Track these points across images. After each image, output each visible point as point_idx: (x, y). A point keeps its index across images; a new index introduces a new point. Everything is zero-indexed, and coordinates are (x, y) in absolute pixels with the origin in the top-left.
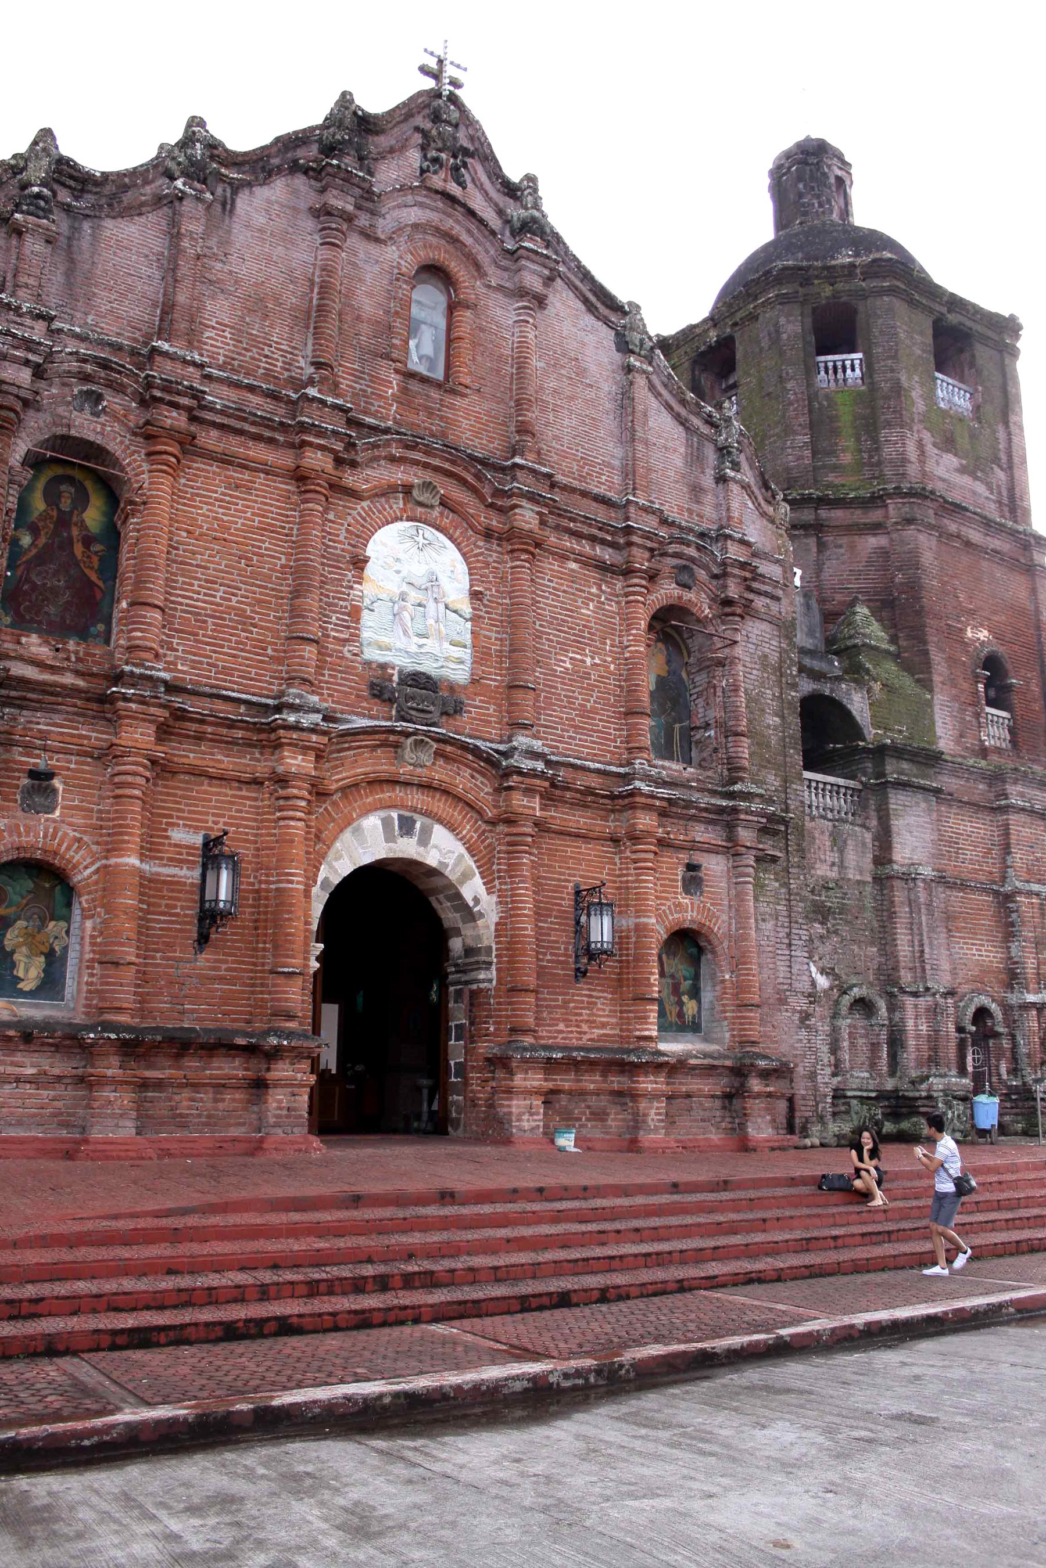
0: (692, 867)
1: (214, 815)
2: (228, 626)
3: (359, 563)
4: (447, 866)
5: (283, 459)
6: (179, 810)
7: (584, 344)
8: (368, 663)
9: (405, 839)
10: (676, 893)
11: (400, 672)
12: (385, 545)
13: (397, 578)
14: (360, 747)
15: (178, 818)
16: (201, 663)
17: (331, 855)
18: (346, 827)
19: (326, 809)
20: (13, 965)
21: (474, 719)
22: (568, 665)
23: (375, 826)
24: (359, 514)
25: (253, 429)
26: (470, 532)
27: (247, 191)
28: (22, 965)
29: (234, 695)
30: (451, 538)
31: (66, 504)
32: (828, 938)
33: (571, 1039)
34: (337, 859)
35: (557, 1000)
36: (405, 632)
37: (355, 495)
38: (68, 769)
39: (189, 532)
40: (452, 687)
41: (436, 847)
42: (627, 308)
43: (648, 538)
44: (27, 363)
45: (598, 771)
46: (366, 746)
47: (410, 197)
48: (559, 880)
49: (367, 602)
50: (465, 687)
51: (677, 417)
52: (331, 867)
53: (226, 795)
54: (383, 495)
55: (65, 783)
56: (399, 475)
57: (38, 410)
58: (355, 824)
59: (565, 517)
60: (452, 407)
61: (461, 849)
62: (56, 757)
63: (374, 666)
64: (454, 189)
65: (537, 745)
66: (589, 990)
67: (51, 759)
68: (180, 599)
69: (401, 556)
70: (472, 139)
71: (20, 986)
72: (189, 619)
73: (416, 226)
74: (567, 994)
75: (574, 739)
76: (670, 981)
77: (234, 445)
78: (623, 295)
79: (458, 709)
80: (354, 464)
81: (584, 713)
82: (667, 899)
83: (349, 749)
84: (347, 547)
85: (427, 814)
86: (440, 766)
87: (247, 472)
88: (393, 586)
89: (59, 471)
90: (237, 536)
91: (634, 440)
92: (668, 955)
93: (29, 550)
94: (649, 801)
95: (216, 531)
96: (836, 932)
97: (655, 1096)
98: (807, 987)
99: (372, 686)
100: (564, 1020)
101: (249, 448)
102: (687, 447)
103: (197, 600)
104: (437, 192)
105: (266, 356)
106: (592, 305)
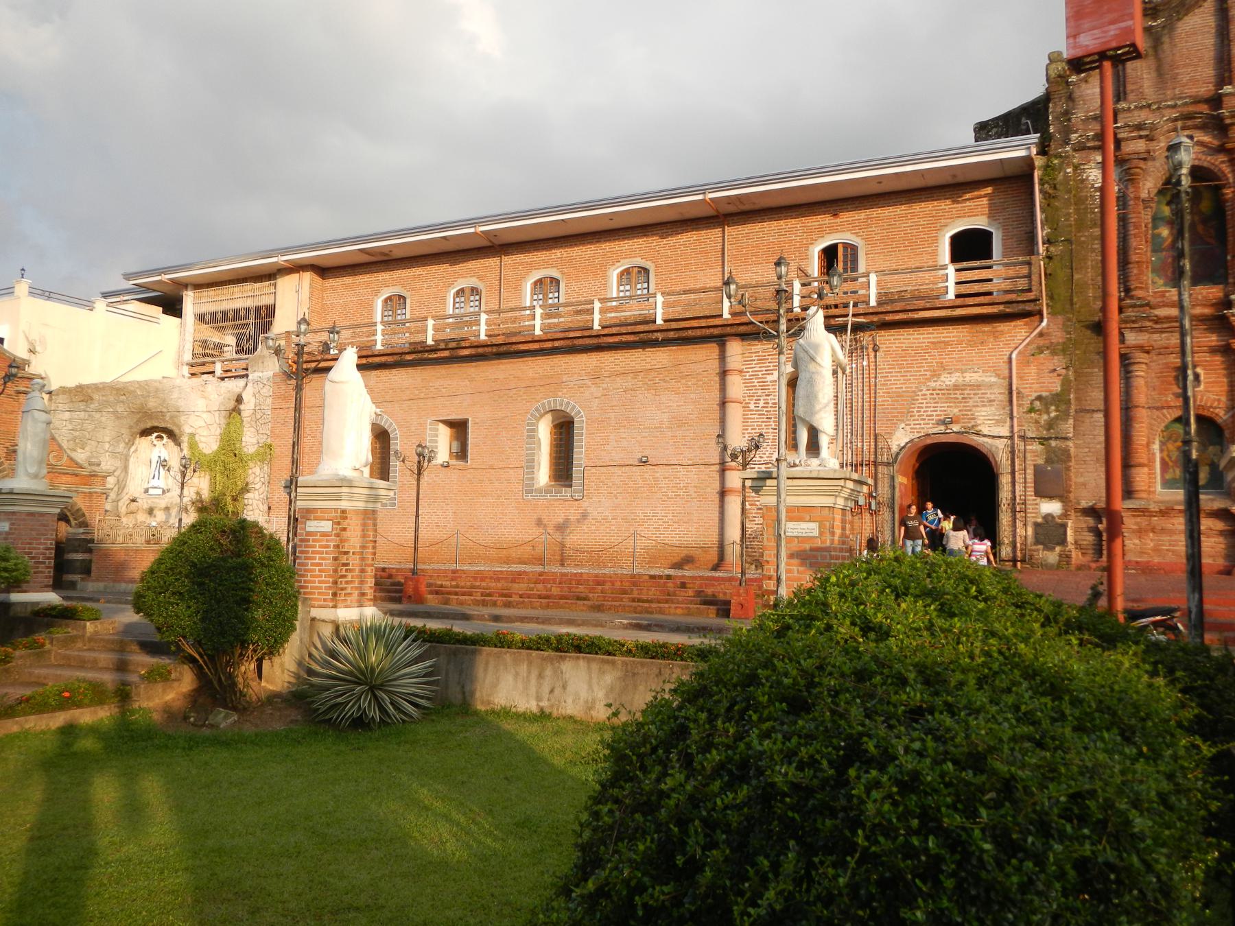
44: (1141, 137)
55: (1205, 369)
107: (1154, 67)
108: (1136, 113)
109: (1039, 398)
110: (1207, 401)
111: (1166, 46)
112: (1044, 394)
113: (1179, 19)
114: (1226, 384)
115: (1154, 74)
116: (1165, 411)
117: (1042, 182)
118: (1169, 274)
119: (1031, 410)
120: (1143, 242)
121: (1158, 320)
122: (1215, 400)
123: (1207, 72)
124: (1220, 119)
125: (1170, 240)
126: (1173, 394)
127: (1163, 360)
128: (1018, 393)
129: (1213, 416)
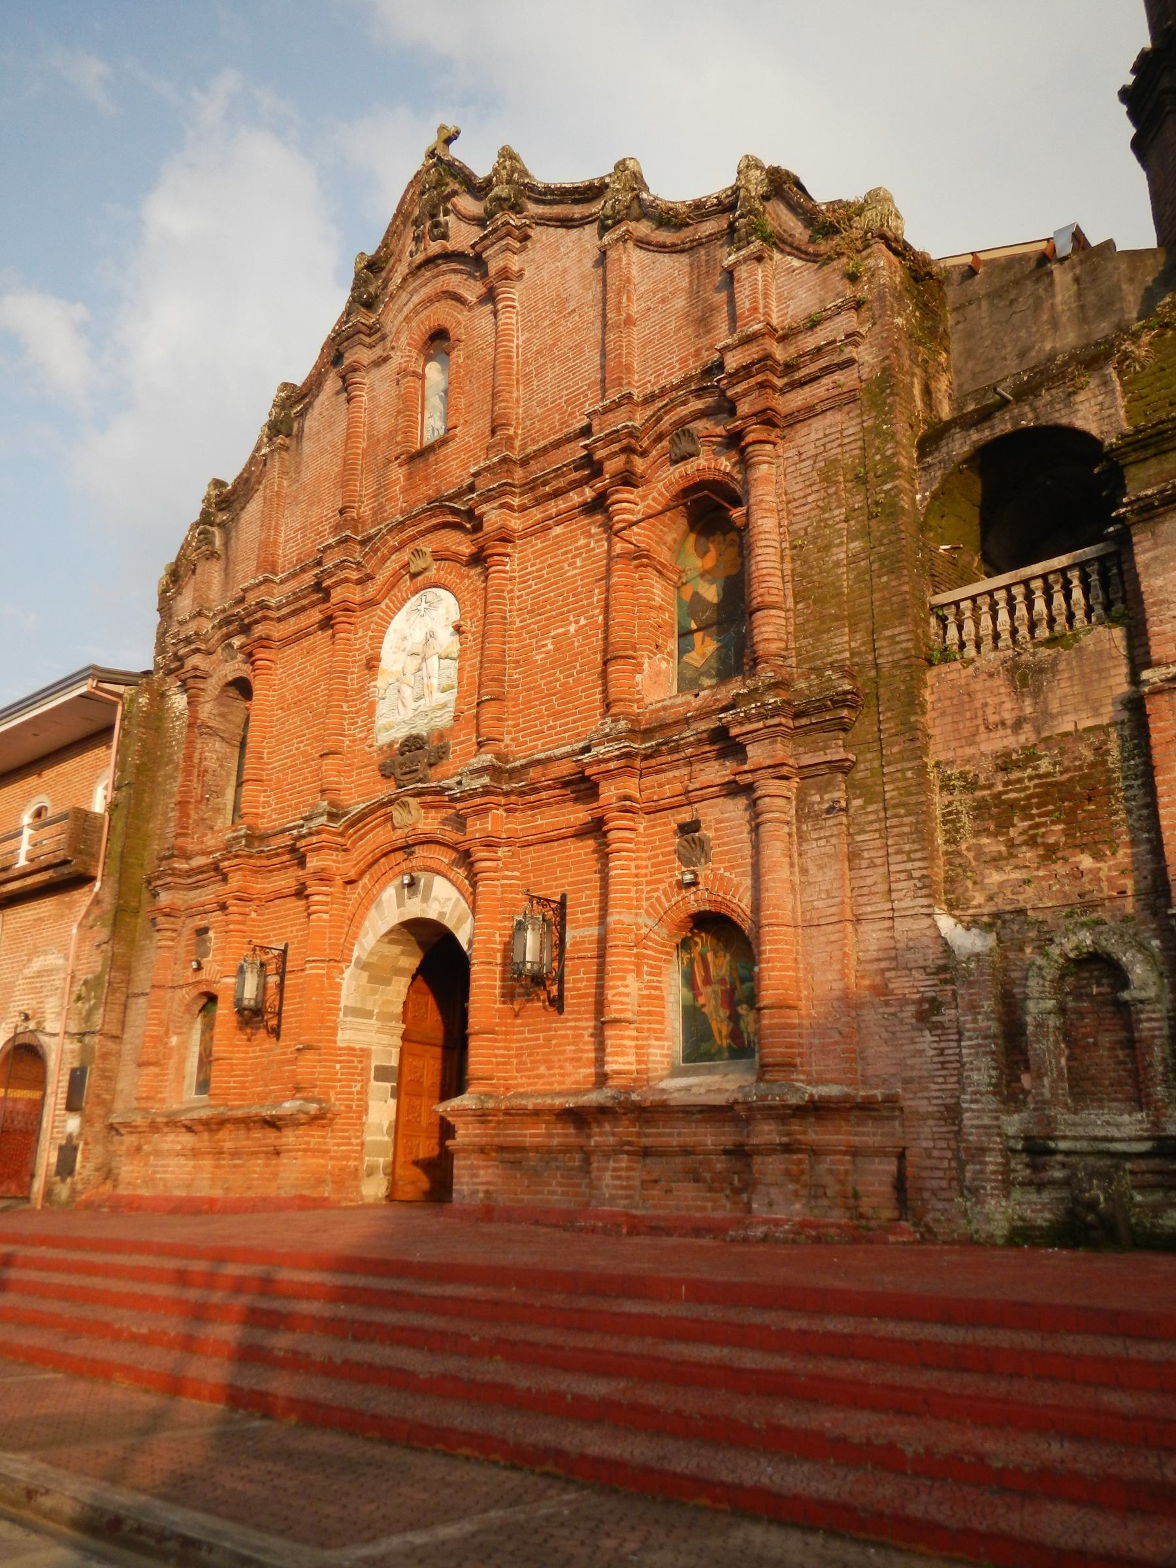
0: (688, 829)
3: (372, 664)
8: (381, 748)
17: (362, 933)
18: (370, 904)
22: (550, 647)
23: (391, 896)
32: (1012, 856)
33: (551, 1084)
35: (537, 1039)
37: (371, 603)
39: (282, 708)
40: (441, 736)
41: (436, 899)
43: (612, 442)
49: (382, 691)
50: (451, 729)
52: (361, 944)
54: (393, 586)
66: (575, 1020)
73: (407, 319)
74: (550, 1029)
76: (718, 988)
79: (442, 753)
80: (370, 577)
82: (661, 881)
85: (427, 869)
86: (433, 818)
92: (716, 956)
94: (603, 767)
96: (1032, 842)
98: (933, 957)
100: (546, 1061)
101: (310, 617)
109: (86, 983)
111: (233, 541)
112: (90, 976)
113: (243, 508)
116: (184, 990)
117: (123, 720)
119: (79, 998)
121: (190, 873)
128: (73, 977)
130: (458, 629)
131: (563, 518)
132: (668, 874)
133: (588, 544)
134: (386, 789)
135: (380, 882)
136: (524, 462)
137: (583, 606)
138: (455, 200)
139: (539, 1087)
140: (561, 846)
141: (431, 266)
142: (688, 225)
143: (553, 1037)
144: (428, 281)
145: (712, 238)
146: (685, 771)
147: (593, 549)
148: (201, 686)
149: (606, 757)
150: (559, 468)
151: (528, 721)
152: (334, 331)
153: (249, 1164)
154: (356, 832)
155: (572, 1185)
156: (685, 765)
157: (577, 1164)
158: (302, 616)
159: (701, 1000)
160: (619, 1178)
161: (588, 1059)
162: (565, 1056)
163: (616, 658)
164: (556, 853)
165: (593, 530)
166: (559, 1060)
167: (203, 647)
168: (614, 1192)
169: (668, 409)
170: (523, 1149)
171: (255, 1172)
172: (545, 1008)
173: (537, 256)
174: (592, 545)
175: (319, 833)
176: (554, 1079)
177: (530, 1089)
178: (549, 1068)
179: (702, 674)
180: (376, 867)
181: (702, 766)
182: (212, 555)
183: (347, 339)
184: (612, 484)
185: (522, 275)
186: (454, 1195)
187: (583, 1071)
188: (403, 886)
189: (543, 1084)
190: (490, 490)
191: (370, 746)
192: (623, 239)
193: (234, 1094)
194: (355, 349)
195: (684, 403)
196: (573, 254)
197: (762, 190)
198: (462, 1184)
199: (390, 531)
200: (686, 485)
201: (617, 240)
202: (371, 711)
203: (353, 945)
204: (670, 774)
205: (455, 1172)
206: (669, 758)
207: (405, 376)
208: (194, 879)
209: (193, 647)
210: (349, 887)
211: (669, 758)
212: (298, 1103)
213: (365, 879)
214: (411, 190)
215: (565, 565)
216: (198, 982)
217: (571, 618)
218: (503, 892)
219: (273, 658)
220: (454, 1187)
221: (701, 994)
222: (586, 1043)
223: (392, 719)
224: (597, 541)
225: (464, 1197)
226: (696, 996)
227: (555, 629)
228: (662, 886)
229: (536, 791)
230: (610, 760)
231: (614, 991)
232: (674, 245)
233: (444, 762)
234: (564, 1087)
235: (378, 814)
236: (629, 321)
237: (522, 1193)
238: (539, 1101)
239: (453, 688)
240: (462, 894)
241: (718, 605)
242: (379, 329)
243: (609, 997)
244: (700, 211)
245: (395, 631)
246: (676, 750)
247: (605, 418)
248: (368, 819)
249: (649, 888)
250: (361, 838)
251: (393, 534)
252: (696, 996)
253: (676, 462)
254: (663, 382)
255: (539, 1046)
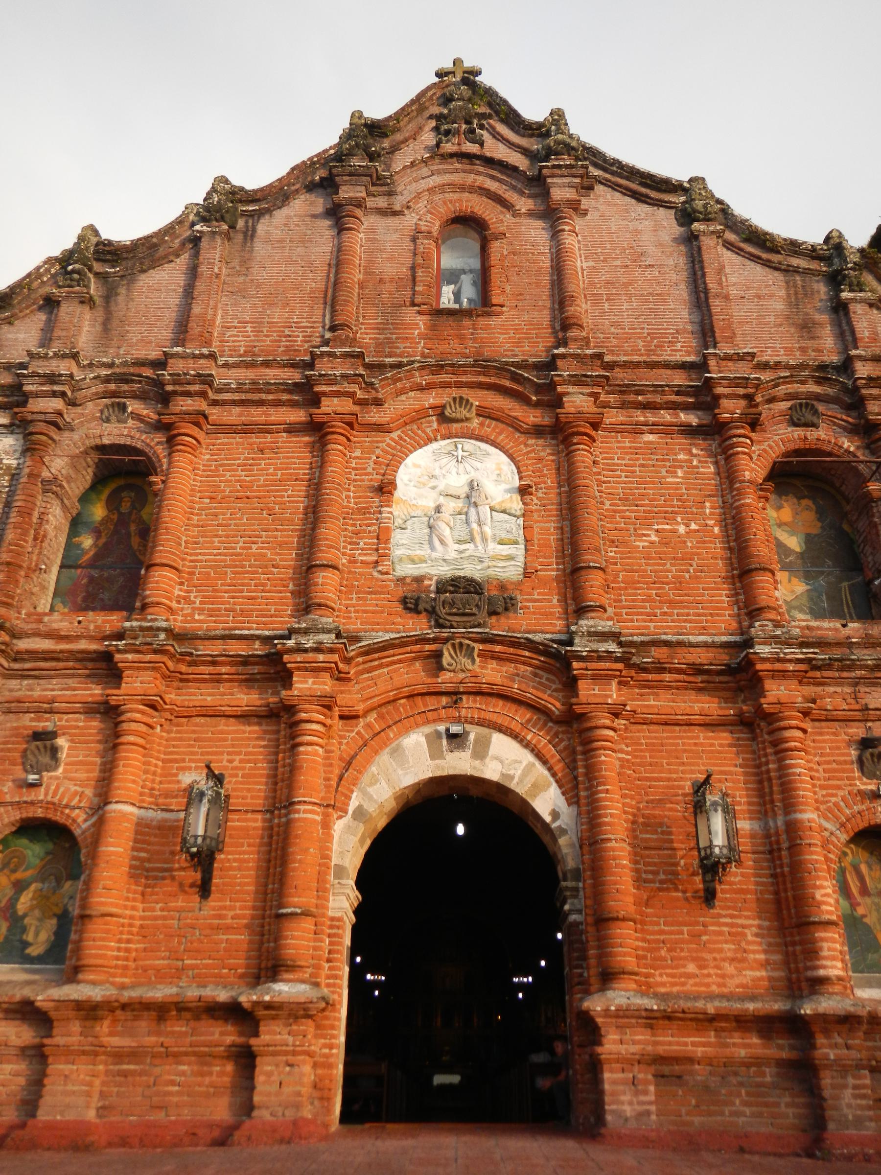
1: (229, 753)
2: (248, 572)
4: (512, 778)
5: (299, 416)
6: (193, 753)
7: (637, 232)
8: (401, 580)
9: (457, 754)
10: (854, 779)
11: (438, 583)
12: (418, 466)
13: (434, 494)
14: (394, 663)
15: (191, 761)
16: (219, 610)
17: (365, 779)
18: (381, 748)
19: (358, 733)
20: (24, 930)
21: (534, 613)
22: (654, 538)
23: (418, 743)
24: (388, 445)
25: (271, 397)
26: (517, 435)
27: (267, 217)
28: (33, 929)
29: (246, 632)
30: (494, 444)
31: (125, 507)
33: (708, 985)
34: (371, 784)
35: (682, 933)
36: (442, 542)
37: (381, 428)
38: (78, 727)
39: (211, 498)
40: (502, 586)
41: (497, 758)
42: (686, 185)
44: (54, 394)
45: (706, 645)
46: (400, 661)
47: (425, 169)
48: (669, 779)
49: (398, 522)
50: (520, 583)
51: (767, 264)
52: (365, 793)
53: (244, 732)
54: (413, 421)
55: (72, 741)
56: (431, 399)
57: (73, 430)
58: (394, 745)
59: (630, 392)
60: (487, 328)
61: (527, 757)
62: (65, 717)
63: (408, 581)
64: (471, 148)
65: (604, 625)
66: (732, 916)
67: (60, 720)
68: (200, 557)
69: (437, 472)
70: (490, 105)
71: (28, 951)
72: (208, 574)
74: (697, 923)
75: (671, 615)
77: (256, 415)
78: (680, 174)
80: (378, 402)
81: (679, 584)
82: (839, 787)
83: (381, 666)
84: (375, 476)
85: (481, 723)
86: (492, 669)
87: (269, 436)
88: (429, 502)
89: (121, 482)
90: (259, 491)
91: (707, 298)
92: (870, 867)
93: (90, 550)
94: (778, 666)
95: (238, 491)
97: (844, 1069)
99: (404, 601)
100: (694, 959)
101: (270, 415)
102: (788, 287)
103: (220, 554)
104: (452, 155)
105: (286, 336)
106: (642, 195)
107: (100, 320)
108: (54, 363)
110: (63, 795)
111: (121, 299)
113: (143, 271)
114: (98, 768)
115: (99, 328)
118: (79, 599)
120: (30, 539)
122: (76, 793)
123: (164, 333)
124: (159, 383)
125: (92, 553)
126: (14, 781)
127: (12, 722)
129: (69, 823)
130: (523, 491)
131: (655, 428)
132: (848, 782)
133: (691, 461)
134: (418, 626)
135: (406, 724)
136: (610, 366)
137: (692, 513)
138: (491, 121)
139: (688, 987)
140: (685, 731)
141: (465, 161)
142: (779, 253)
143: (705, 933)
144: (456, 171)
145: (807, 272)
146: (847, 689)
147: (697, 467)
148: (56, 437)
149: (788, 657)
150: (662, 386)
151: (634, 600)
152: (311, 159)
153: (157, 1070)
154: (363, 663)
155: (767, 1105)
156: (850, 685)
157: (768, 1079)
158: (253, 410)
159: (860, 911)
160: (864, 1097)
161: (755, 960)
162: (723, 955)
163: (765, 569)
164: (681, 738)
165: (694, 451)
166: (715, 959)
167: (69, 393)
168: (859, 1112)
169: (786, 380)
170: (690, 1060)
171: (173, 1083)
172: (687, 899)
173: (601, 208)
174: (695, 463)
175: (331, 651)
176: (710, 980)
177: (675, 989)
178: (701, 967)
179: (795, 608)
180: (390, 707)
181: (867, 690)
182: (88, 301)
183: (351, 174)
184: (739, 420)
185: (586, 214)
186: (609, 1118)
187: (748, 973)
188: (438, 734)
189: (696, 985)
190: (586, 376)
191: (387, 573)
192: (719, 235)
193: (116, 967)
194: (359, 188)
195: (803, 382)
196: (647, 222)
197: (856, 258)
198: (623, 1103)
199: (422, 368)
200: (802, 446)
201: (712, 233)
202: (382, 537)
203: (352, 792)
204: (832, 689)
205: (607, 1087)
206: (837, 674)
207: (426, 238)
208: (28, 665)
209: (56, 388)
210: (341, 722)
211: (837, 674)
212: (303, 987)
213: (372, 718)
214: (433, 91)
215: (664, 471)
216: (32, 803)
217: (679, 519)
218: (622, 767)
219: (201, 440)
220: (607, 1107)
221: (859, 904)
222: (749, 943)
223: (419, 552)
224: (700, 462)
225: (626, 1120)
226: (854, 905)
227: (658, 524)
228: (841, 793)
229: (661, 670)
230: (790, 661)
231: (823, 891)
232: (769, 261)
233: (511, 615)
234: (725, 990)
235: (409, 649)
236: (727, 297)
237: (688, 1113)
238: (717, 1004)
239: (516, 543)
240: (544, 762)
241: (801, 554)
242: (388, 184)
243: (818, 896)
244: (794, 247)
245: (416, 466)
246: (850, 668)
247: (724, 363)
248: (391, 652)
249: (824, 792)
250: (369, 671)
251: (424, 372)
252: (854, 905)
253: (796, 425)
254: (778, 359)
255: (683, 941)
